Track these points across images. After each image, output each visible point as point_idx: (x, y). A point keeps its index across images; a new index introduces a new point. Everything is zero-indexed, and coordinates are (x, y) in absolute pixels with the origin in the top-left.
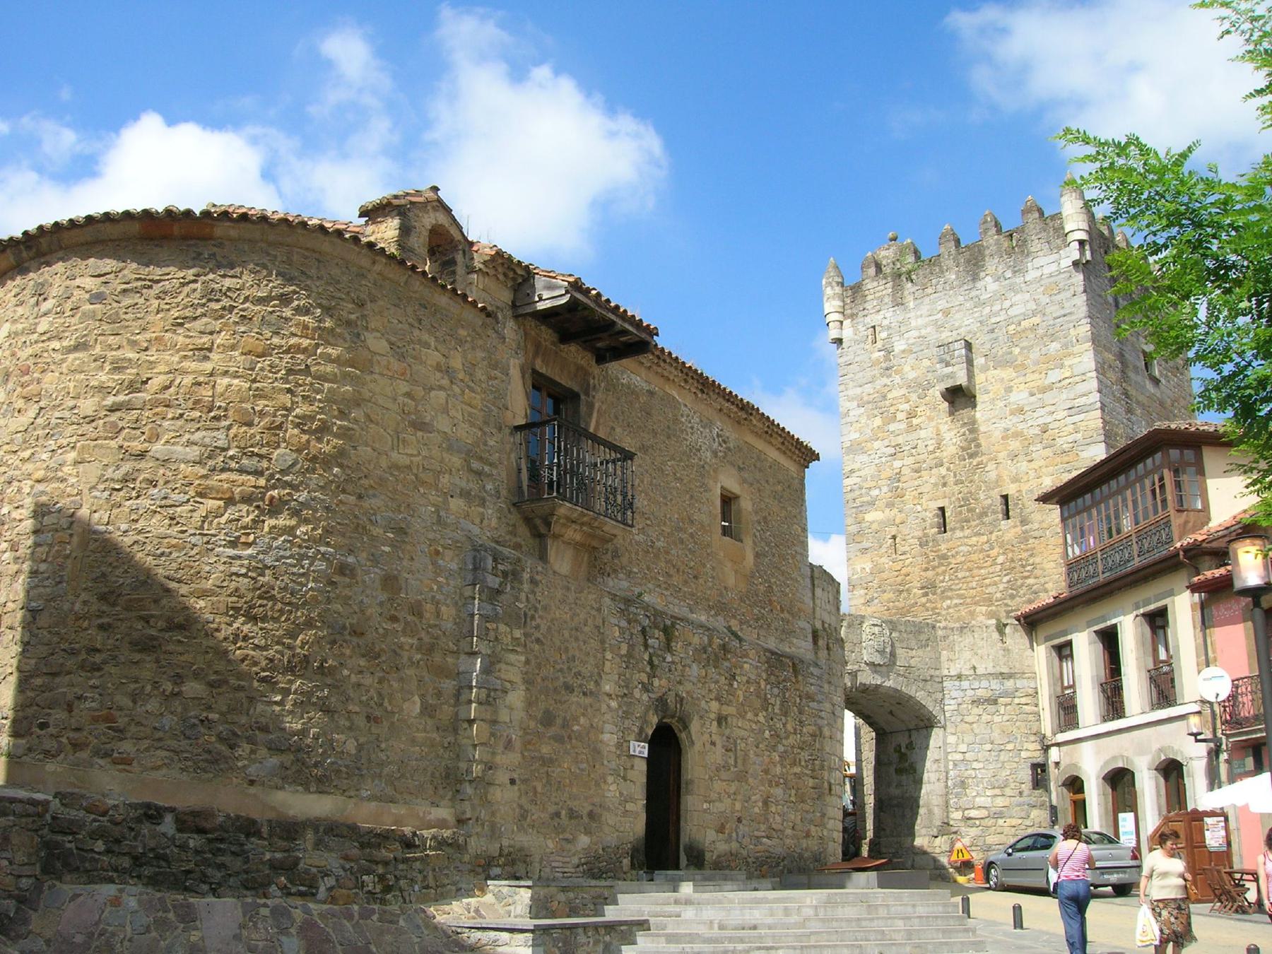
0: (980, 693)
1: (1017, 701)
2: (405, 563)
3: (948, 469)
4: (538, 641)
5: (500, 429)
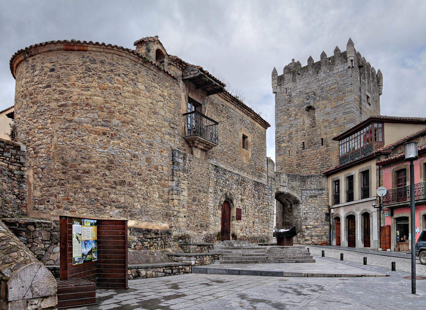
2: (152, 154)
3: (306, 131)
4: (191, 177)
5: (179, 115)
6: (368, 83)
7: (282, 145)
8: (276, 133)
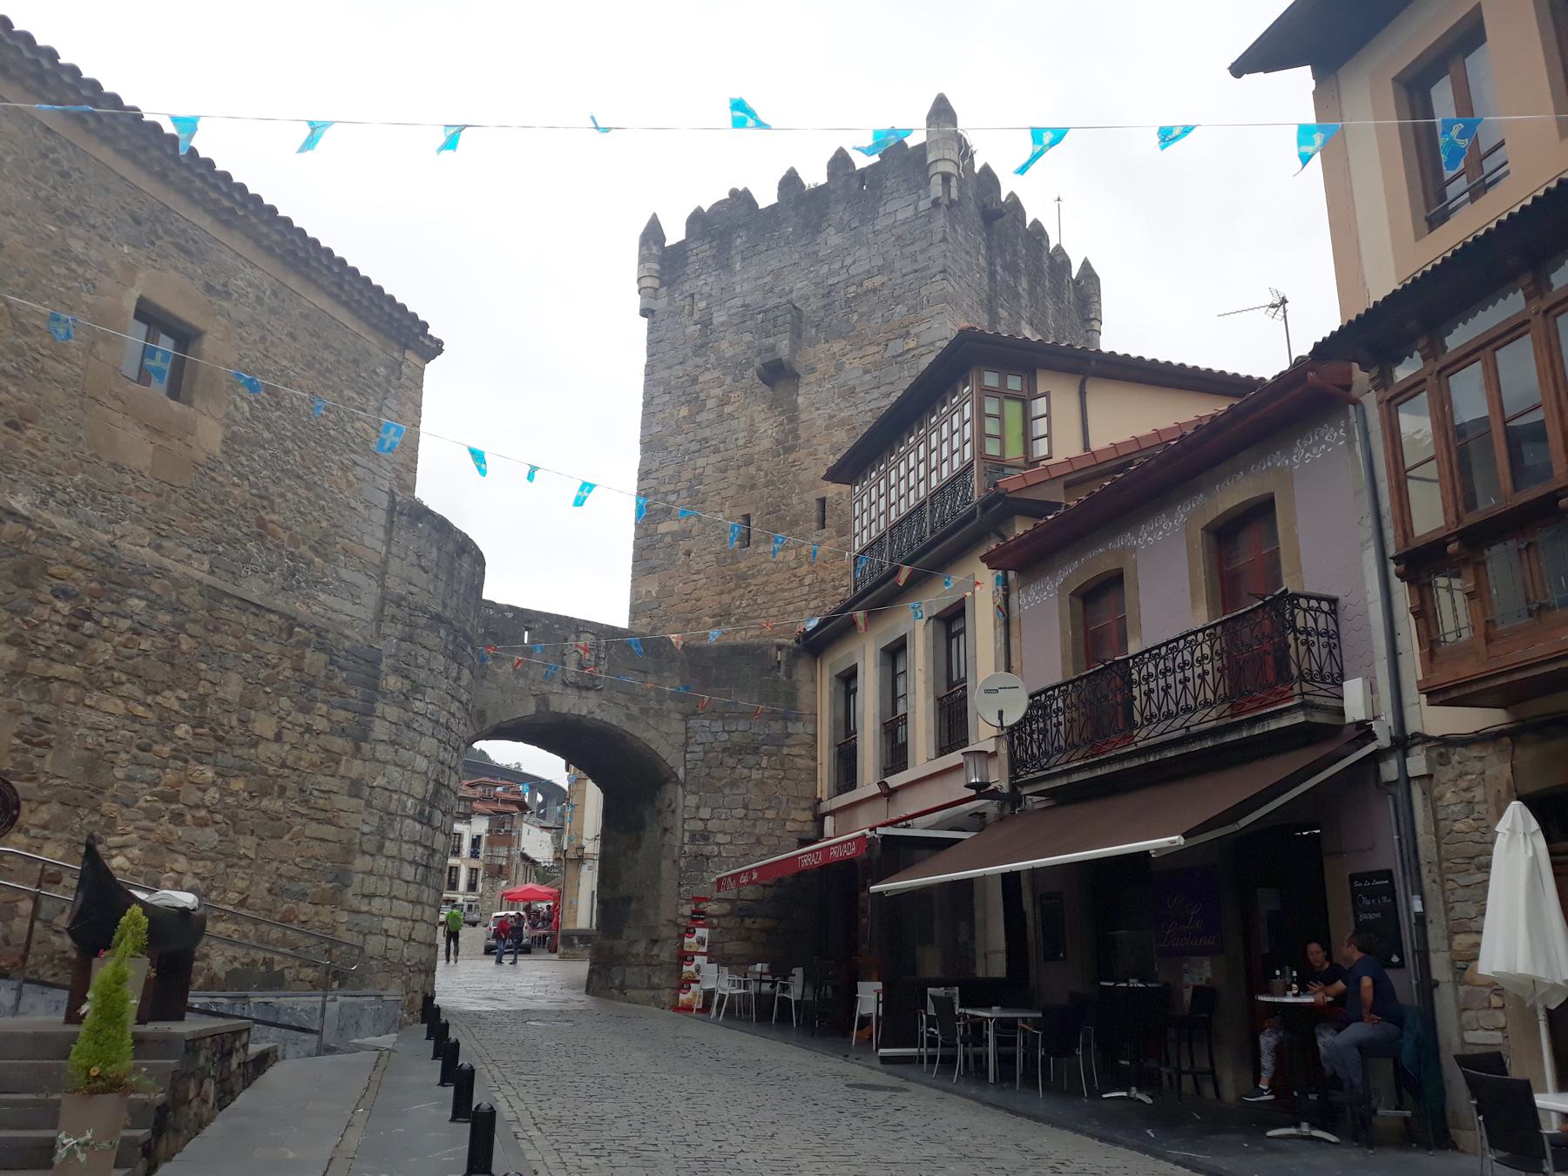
0: (736, 737)
1: (785, 751)
3: (759, 469)
6: (1032, 291)
7: (662, 528)
8: (641, 479)
